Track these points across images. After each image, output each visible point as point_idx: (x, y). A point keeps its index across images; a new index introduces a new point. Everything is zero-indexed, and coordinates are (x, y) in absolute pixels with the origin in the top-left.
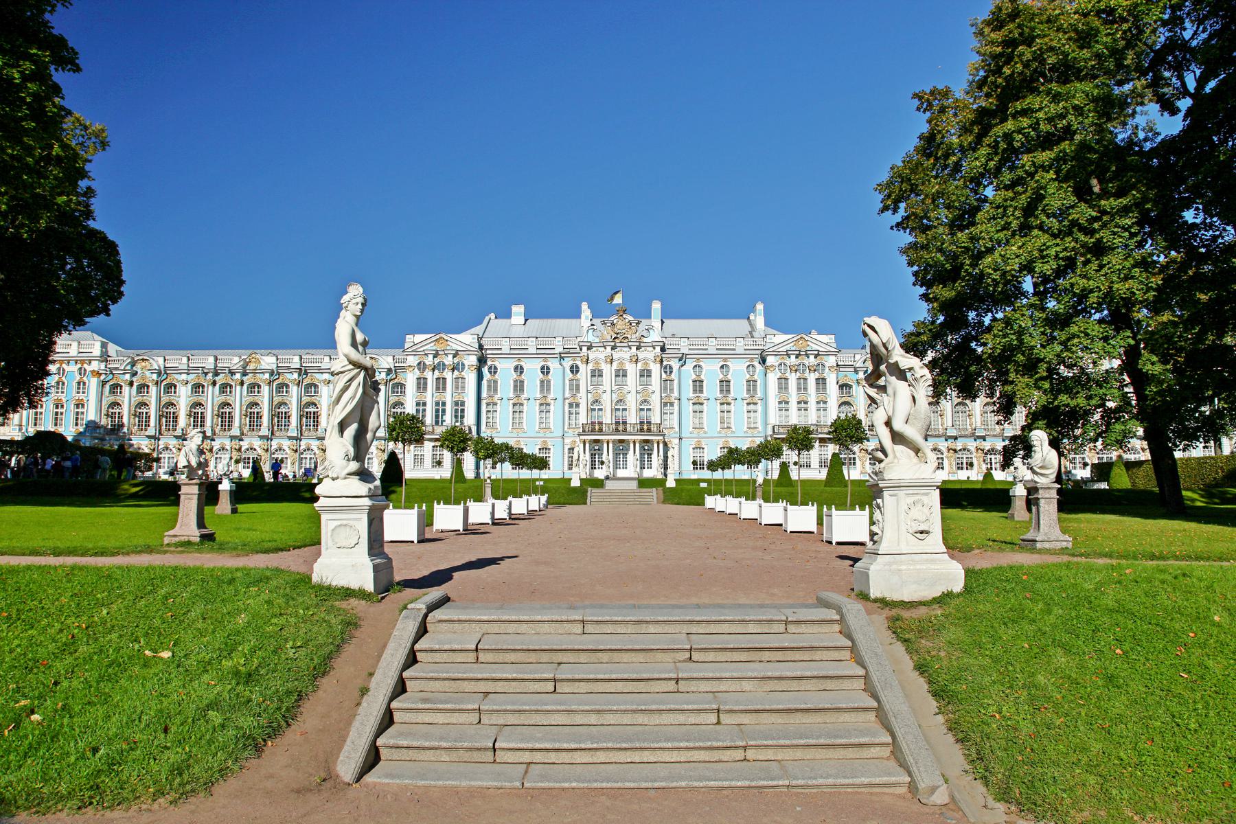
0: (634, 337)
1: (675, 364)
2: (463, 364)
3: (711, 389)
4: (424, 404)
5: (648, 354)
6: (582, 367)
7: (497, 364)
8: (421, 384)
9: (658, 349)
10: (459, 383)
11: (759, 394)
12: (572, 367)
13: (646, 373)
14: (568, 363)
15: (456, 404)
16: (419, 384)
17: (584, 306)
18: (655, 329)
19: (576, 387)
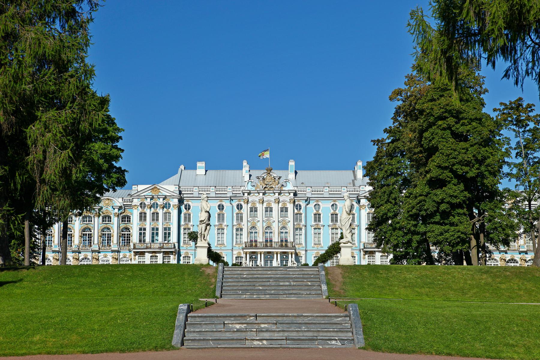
0: (277, 187)
1: (303, 204)
2: (169, 204)
3: (326, 219)
4: (145, 229)
5: (286, 198)
6: (244, 206)
7: (190, 203)
8: (142, 217)
9: (292, 195)
10: (167, 216)
11: (356, 223)
12: (238, 206)
13: (284, 210)
14: (235, 203)
15: (165, 229)
16: (141, 217)
17: (245, 163)
18: (290, 178)
19: (240, 218)
